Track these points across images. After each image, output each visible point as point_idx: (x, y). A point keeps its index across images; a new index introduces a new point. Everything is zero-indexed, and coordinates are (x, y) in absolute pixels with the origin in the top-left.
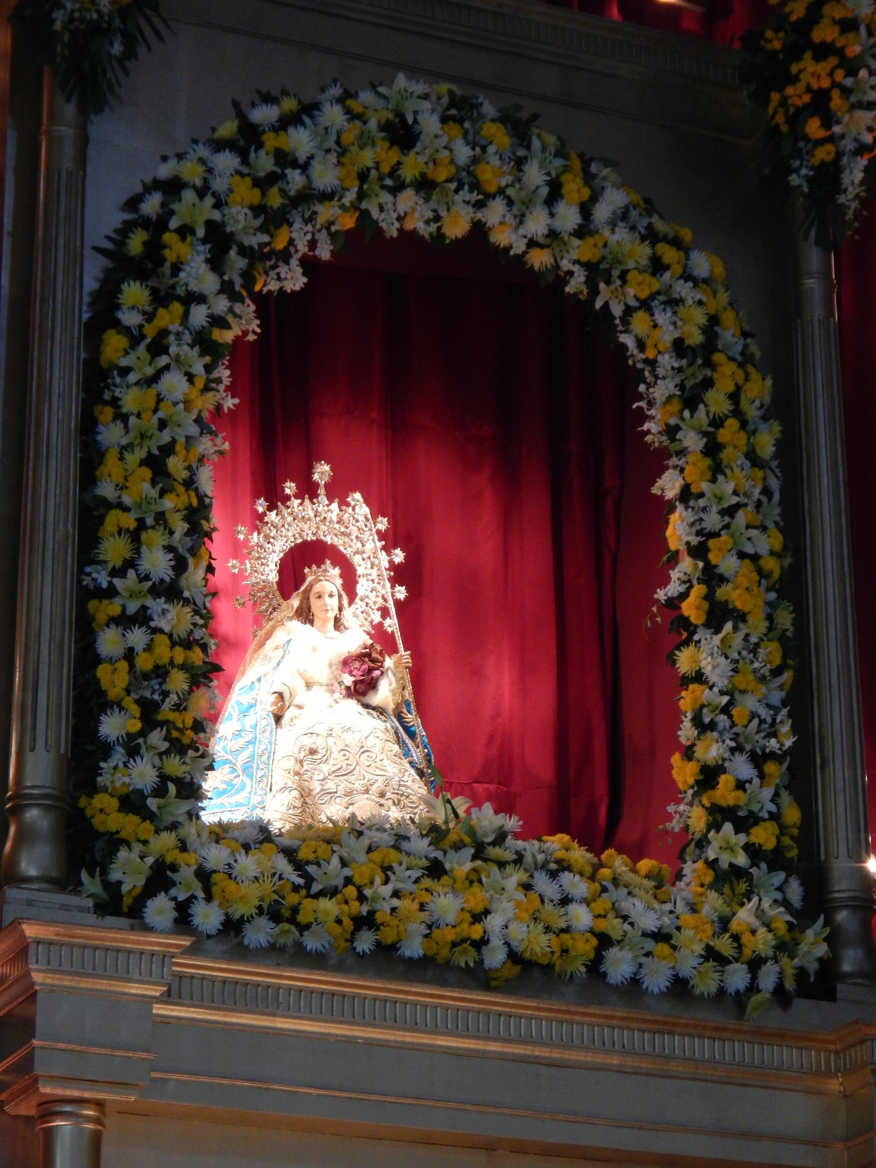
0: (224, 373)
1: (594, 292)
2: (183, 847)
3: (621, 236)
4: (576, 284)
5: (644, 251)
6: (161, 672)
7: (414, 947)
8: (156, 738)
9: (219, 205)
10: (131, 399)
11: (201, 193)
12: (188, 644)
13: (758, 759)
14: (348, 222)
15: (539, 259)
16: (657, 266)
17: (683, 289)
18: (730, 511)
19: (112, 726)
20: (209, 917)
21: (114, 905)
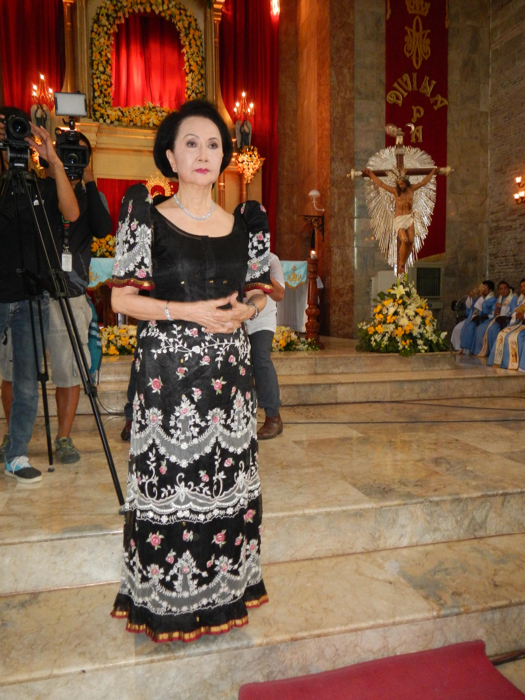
0: (112, 38)
1: (171, 20)
2: (106, 111)
3: (173, 9)
4: (168, 18)
5: (178, 12)
6: (102, 86)
7: (139, 124)
8: (102, 95)
9: (108, 10)
10: (97, 43)
11: (105, 8)
12: (107, 81)
13: (196, 94)
14: (131, 11)
15: (163, 14)
16: (180, 14)
17: (184, 18)
18: (192, 55)
19: (96, 94)
20: (108, 121)
21: (97, 120)
